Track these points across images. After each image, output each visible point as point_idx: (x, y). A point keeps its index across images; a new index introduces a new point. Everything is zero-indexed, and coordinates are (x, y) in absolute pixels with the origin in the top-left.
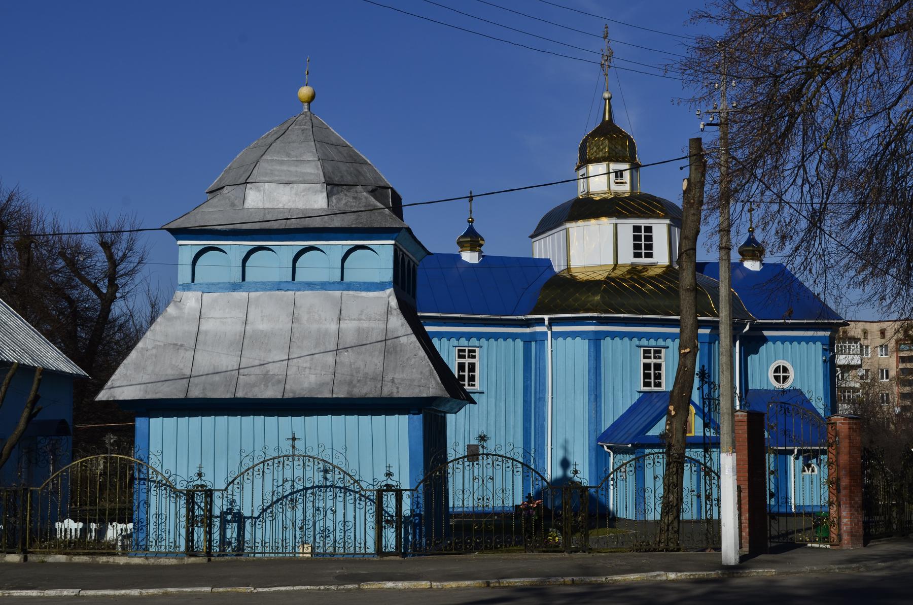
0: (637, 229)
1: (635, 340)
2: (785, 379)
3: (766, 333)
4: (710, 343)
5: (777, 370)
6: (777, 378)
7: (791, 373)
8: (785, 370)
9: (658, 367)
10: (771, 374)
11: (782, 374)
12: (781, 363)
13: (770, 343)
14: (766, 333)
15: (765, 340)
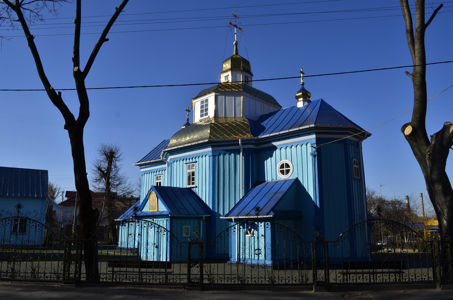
0: (202, 102)
1: (185, 161)
2: (288, 171)
3: (275, 144)
4: (214, 156)
5: (282, 166)
6: (282, 172)
7: (291, 168)
8: (287, 166)
9: (193, 174)
10: (278, 169)
11: (285, 169)
12: (284, 161)
13: (278, 151)
14: (275, 144)
15: (275, 148)
